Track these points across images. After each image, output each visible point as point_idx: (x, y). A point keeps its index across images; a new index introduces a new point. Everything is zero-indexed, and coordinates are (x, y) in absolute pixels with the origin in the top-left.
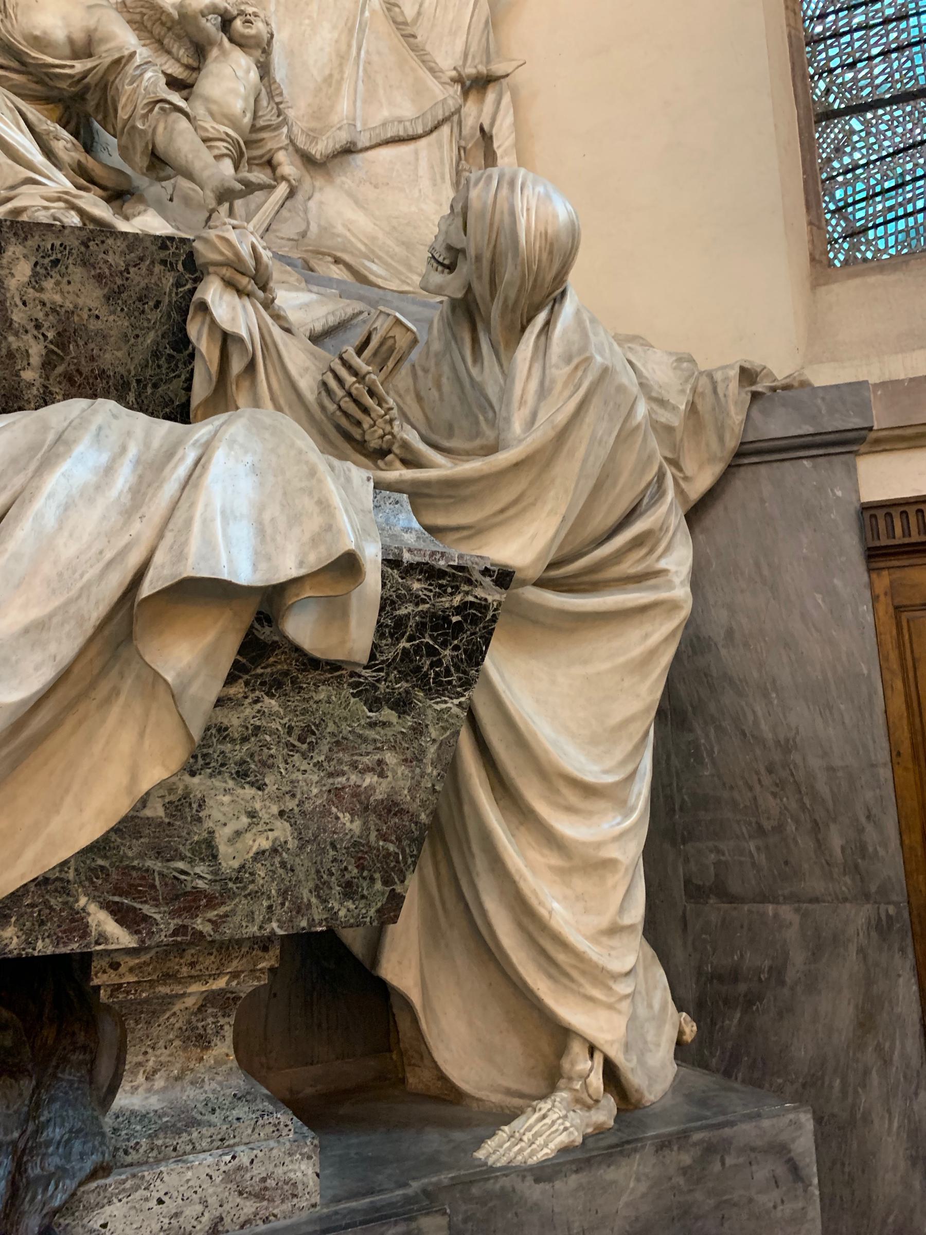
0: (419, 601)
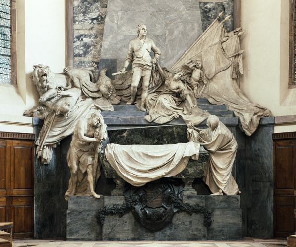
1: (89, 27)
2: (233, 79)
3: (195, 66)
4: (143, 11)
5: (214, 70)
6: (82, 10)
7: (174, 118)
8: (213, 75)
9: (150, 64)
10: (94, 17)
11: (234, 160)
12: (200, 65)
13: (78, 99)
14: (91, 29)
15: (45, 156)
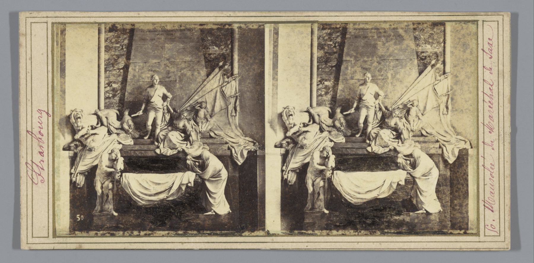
7: (179, 152)
10: (121, 67)
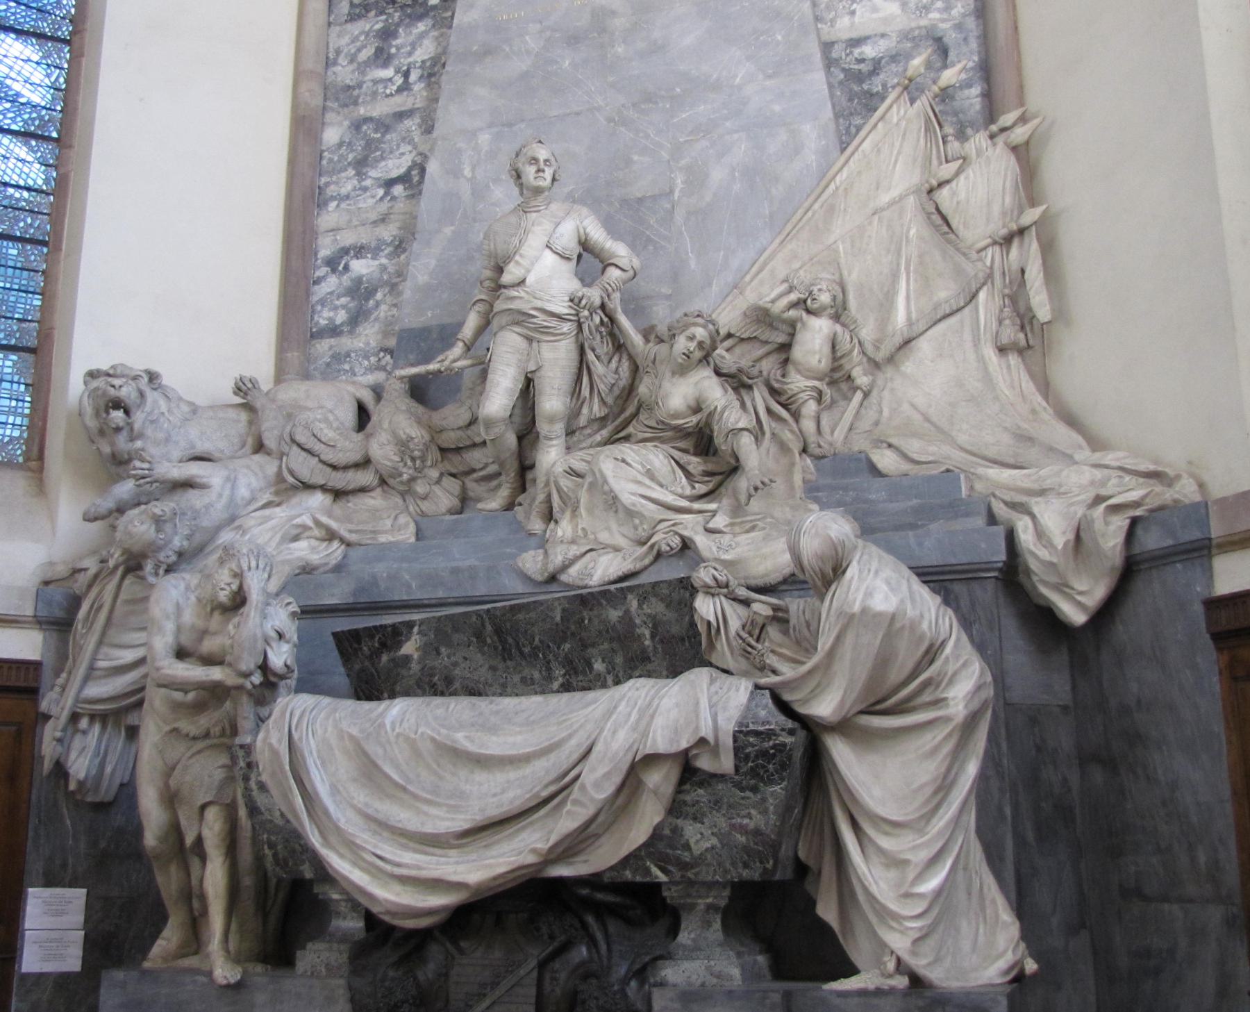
0: (753, 746)
1: (373, 216)
2: (1002, 350)
3: (800, 304)
4: (578, 114)
5: (900, 317)
6: (351, 157)
7: (659, 555)
8: (898, 340)
9: (562, 308)
10: (394, 174)
11: (972, 769)
12: (825, 298)
13: (253, 499)
14: (383, 220)
15: (80, 766)
